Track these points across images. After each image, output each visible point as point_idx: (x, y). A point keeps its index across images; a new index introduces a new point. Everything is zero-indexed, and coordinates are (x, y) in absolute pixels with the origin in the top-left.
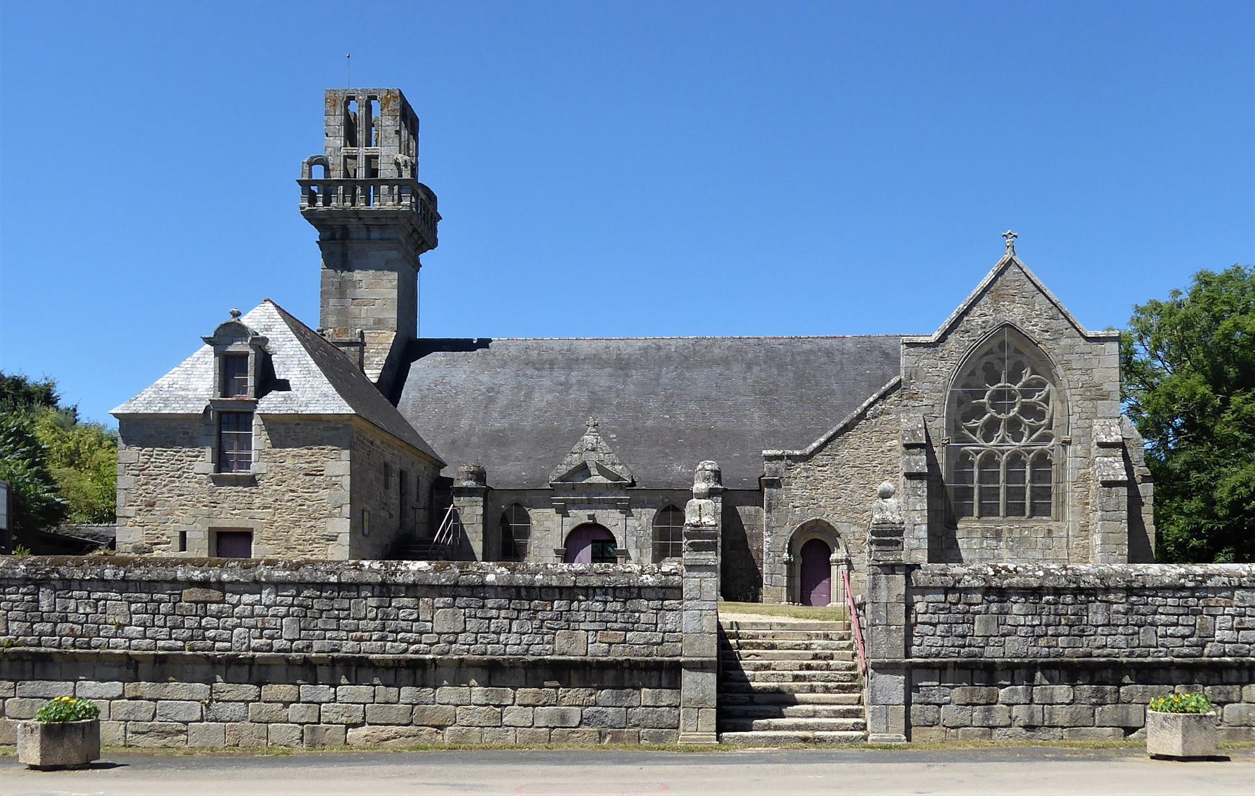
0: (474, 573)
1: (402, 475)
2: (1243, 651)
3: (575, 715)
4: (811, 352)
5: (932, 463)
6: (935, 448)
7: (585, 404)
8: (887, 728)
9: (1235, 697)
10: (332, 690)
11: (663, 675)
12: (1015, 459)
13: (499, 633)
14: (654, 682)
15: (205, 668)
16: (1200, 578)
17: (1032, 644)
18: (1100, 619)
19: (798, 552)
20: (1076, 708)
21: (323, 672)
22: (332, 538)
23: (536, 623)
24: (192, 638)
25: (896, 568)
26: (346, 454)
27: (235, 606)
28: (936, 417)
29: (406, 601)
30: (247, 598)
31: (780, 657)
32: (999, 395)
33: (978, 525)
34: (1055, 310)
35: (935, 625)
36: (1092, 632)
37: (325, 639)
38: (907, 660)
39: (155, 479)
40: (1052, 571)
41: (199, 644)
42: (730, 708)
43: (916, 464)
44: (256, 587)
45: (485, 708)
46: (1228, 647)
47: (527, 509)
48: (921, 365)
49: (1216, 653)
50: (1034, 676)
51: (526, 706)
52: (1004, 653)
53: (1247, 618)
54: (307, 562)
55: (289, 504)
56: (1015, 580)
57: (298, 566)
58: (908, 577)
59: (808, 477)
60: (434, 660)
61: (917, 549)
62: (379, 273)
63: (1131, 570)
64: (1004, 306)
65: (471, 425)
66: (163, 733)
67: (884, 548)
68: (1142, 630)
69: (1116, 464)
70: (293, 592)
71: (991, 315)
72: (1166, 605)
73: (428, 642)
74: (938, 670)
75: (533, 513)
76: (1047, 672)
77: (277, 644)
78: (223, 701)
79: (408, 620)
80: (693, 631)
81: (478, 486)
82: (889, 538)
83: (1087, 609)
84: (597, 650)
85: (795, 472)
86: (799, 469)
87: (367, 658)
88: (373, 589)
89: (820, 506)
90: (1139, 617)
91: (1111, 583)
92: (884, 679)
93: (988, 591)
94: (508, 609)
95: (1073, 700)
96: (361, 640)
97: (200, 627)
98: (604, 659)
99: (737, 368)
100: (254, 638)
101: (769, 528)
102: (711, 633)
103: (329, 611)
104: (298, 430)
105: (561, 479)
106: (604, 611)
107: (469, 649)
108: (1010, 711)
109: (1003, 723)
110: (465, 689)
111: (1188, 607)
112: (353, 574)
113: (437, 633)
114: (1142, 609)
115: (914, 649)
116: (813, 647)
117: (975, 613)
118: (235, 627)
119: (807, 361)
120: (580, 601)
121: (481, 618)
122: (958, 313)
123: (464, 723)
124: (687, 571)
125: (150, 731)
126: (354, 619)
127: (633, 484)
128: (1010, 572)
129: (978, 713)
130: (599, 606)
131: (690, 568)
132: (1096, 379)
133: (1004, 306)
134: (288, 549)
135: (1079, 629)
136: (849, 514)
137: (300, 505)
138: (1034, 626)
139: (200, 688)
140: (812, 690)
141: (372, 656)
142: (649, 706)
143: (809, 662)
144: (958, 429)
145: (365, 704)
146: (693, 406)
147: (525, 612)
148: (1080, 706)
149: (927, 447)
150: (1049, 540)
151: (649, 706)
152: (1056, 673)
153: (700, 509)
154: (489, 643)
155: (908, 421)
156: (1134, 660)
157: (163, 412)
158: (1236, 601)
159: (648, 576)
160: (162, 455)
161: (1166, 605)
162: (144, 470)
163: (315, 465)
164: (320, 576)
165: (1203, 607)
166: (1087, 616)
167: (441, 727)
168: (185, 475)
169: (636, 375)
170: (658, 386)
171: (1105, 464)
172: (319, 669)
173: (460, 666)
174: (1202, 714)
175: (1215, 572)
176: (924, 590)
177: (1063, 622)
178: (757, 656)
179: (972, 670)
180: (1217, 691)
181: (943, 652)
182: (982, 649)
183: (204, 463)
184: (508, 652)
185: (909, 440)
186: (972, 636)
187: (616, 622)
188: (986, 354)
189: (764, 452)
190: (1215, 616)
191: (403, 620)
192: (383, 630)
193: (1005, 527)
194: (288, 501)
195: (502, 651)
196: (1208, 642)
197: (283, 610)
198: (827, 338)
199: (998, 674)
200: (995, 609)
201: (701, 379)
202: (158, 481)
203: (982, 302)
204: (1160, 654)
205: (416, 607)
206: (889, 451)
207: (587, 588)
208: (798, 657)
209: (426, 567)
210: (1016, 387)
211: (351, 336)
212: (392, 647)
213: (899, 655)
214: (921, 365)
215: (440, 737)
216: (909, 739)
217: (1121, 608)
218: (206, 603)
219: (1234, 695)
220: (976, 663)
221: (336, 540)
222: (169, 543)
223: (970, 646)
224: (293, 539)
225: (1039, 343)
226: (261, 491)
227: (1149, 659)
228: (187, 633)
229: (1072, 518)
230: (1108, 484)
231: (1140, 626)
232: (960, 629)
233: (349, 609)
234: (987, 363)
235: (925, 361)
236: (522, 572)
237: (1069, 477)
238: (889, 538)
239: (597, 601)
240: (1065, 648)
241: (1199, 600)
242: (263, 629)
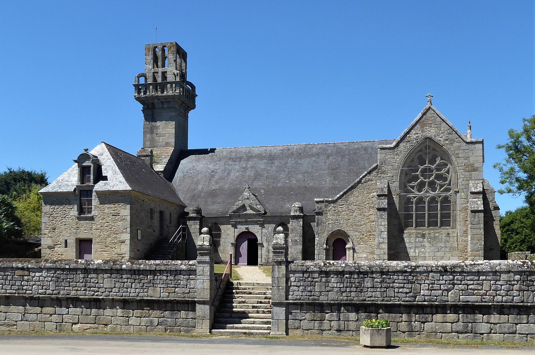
0: (118, 265)
1: (161, 213)
2: (433, 300)
3: (156, 321)
4: (358, 149)
5: (391, 203)
6: (393, 196)
7: (253, 177)
8: (278, 329)
9: (430, 320)
10: (67, 310)
11: (189, 305)
12: (433, 200)
13: (128, 288)
14: (186, 309)
15: (23, 301)
16: (413, 268)
17: (340, 295)
18: (369, 285)
19: (332, 244)
20: (359, 323)
21: (64, 303)
22: (123, 242)
23: (141, 284)
24: (18, 289)
25: (282, 263)
26: (128, 206)
27: (33, 277)
28: (394, 182)
29: (94, 275)
30: (37, 274)
31: (251, 298)
32: (424, 171)
33: (414, 231)
34: (451, 130)
35: (299, 287)
36: (366, 291)
37: (64, 290)
38: (286, 301)
39: (56, 218)
40: (349, 264)
41: (21, 292)
42: (220, 319)
43: (382, 204)
44: (40, 270)
45: (122, 318)
46: (426, 298)
47: (219, 225)
48: (387, 158)
49: (421, 300)
50: (340, 309)
51: (137, 317)
52: (328, 299)
53: (435, 285)
54: (59, 260)
56: (332, 268)
57: (55, 262)
58: (287, 267)
59: (335, 210)
60: (103, 299)
61: (383, 243)
62: (167, 122)
63: (383, 264)
64: (426, 129)
65: (202, 188)
66: (9, 325)
67: (277, 254)
68: (388, 290)
69: (479, 202)
70: (53, 272)
71: (420, 134)
72: (399, 279)
73: (102, 291)
74: (300, 306)
75: (222, 227)
76: (346, 307)
77: (48, 292)
78: (29, 313)
79: (94, 283)
80: (201, 288)
81: (197, 216)
82: (279, 250)
83: (364, 280)
84: (164, 296)
85: (329, 208)
86: (331, 207)
87: (79, 298)
88: (82, 271)
89: (340, 224)
90: (386, 284)
91: (374, 270)
92: (276, 309)
93: (321, 272)
94: (131, 278)
95: (357, 319)
96: (77, 290)
97: (21, 285)
98: (166, 299)
99: (322, 157)
100: (40, 290)
101: (318, 234)
102: (207, 289)
103: (66, 279)
104: (110, 196)
105: (234, 212)
106: (167, 280)
107: (116, 294)
108: (330, 324)
109: (327, 329)
110: (115, 310)
111: (409, 280)
112: (74, 265)
113: (105, 288)
114: (388, 281)
115: (290, 296)
116: (267, 293)
117: (316, 282)
118: (33, 285)
119: (355, 153)
120: (158, 276)
121: (121, 282)
122: (404, 133)
123: (115, 323)
124: (198, 264)
125: (4, 324)
126: (75, 282)
127: (266, 213)
128: (331, 264)
129: (317, 324)
130: (165, 278)
131: (199, 263)
133: (426, 129)
134: (106, 246)
135: (360, 289)
136: (354, 227)
138: (341, 288)
139: (21, 308)
140: (258, 312)
141: (81, 297)
142: (184, 318)
143: (261, 300)
144: (405, 186)
145: (79, 315)
146: (300, 176)
147: (137, 280)
148: (360, 322)
149: (389, 196)
150: (448, 238)
151: (184, 318)
152: (350, 308)
153: (204, 239)
154: (124, 292)
155: (380, 184)
156: (384, 303)
157: (58, 191)
158: (430, 278)
159: (183, 266)
160: (58, 208)
161: (399, 279)
162: (52, 215)
163: (116, 211)
164: (63, 266)
165: (415, 280)
166: (364, 284)
167: (106, 325)
168: (67, 216)
169: (277, 163)
170: (286, 167)
171: (474, 202)
172: (62, 302)
173: (113, 301)
174: (380, 328)
175: (421, 265)
176: (294, 272)
177: (353, 286)
178: (242, 297)
179: (314, 306)
180: (421, 317)
181: (302, 298)
182: (319, 297)
183: (74, 211)
184: (131, 296)
185: (380, 193)
186: (315, 291)
187: (171, 284)
188: (419, 152)
189: (316, 199)
190: (421, 284)
191: (93, 283)
192: (85, 287)
193: (427, 232)
194: (106, 227)
195: (128, 295)
196: (417, 295)
197: (50, 279)
198: (366, 142)
199: (325, 308)
200: (324, 280)
201: (305, 163)
202: (57, 219)
203: (416, 128)
204: (396, 300)
205: (97, 278)
206: (372, 197)
207: (160, 270)
208: (259, 298)
209: (101, 262)
210: (433, 167)
211: (147, 153)
212: (88, 293)
213: (283, 299)
214: (387, 158)
215: (106, 329)
216: (287, 334)
217: (378, 280)
218: (23, 276)
219: (429, 318)
220: (315, 303)
221: (124, 243)
222: (61, 244)
223: (313, 296)
224: (108, 242)
225: (443, 145)
227: (391, 303)
228: (17, 287)
229: (460, 227)
230: (473, 212)
231: (387, 288)
232: (309, 289)
233: (73, 278)
234: (419, 156)
235: (389, 156)
236: (136, 264)
237: (458, 208)
238: (279, 250)
239: (164, 276)
240: (355, 297)
241: (413, 277)
242: (43, 286)
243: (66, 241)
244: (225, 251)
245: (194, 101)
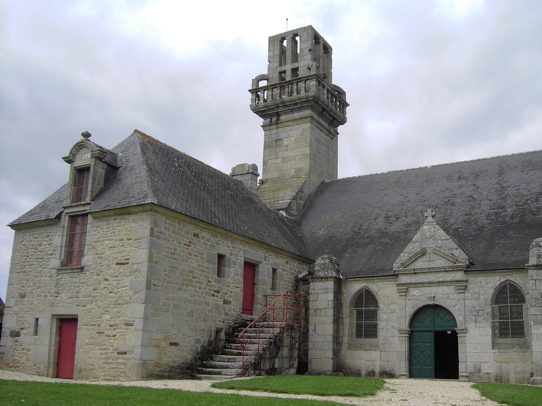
55: (103, 292)
137: (111, 292)
226: (86, 281)
243: (37, 319)
244: (387, 346)
245: (344, 112)
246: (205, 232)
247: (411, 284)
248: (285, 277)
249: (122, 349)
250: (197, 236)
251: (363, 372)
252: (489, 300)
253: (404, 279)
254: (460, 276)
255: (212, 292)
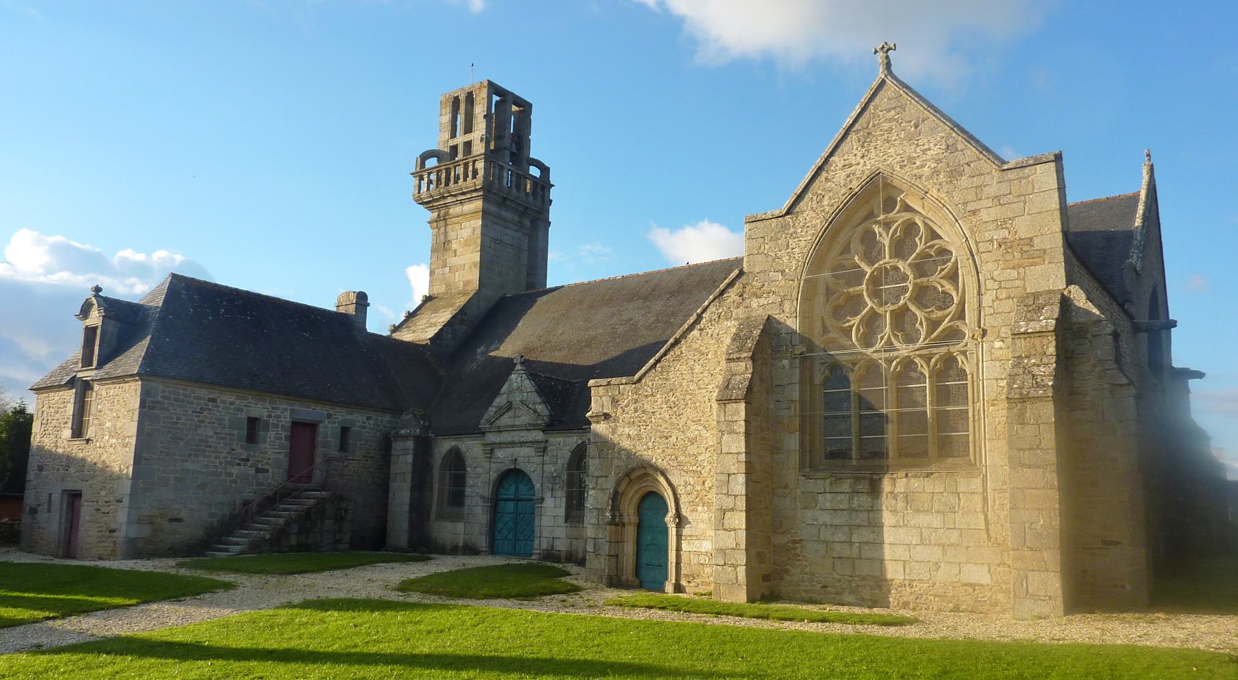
32: (875, 281)
132: (1023, 233)
243: (51, 494)
246: (226, 395)
247: (495, 444)
248: (365, 435)
249: (113, 526)
250: (214, 400)
251: (448, 547)
252: (566, 466)
253: (491, 438)
254: (539, 436)
255: (237, 461)
